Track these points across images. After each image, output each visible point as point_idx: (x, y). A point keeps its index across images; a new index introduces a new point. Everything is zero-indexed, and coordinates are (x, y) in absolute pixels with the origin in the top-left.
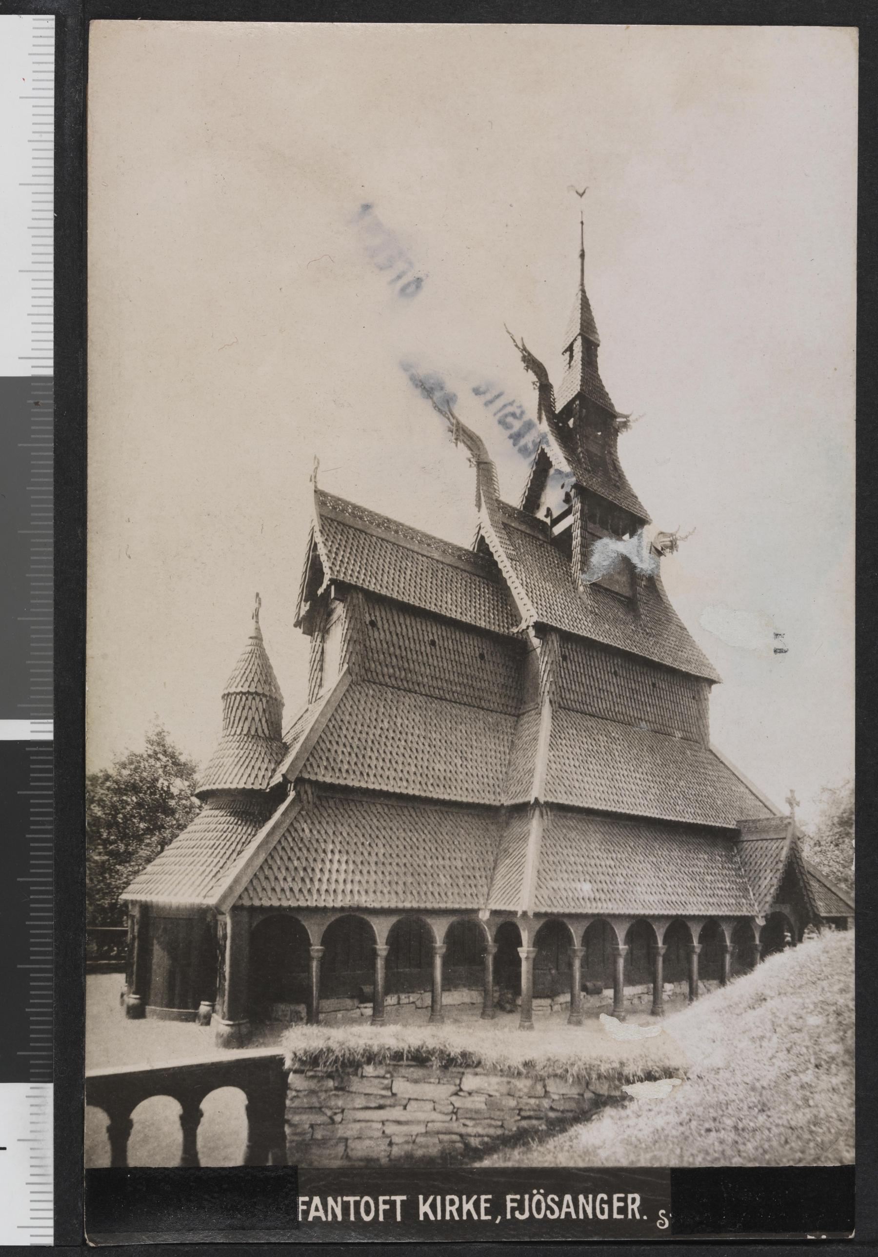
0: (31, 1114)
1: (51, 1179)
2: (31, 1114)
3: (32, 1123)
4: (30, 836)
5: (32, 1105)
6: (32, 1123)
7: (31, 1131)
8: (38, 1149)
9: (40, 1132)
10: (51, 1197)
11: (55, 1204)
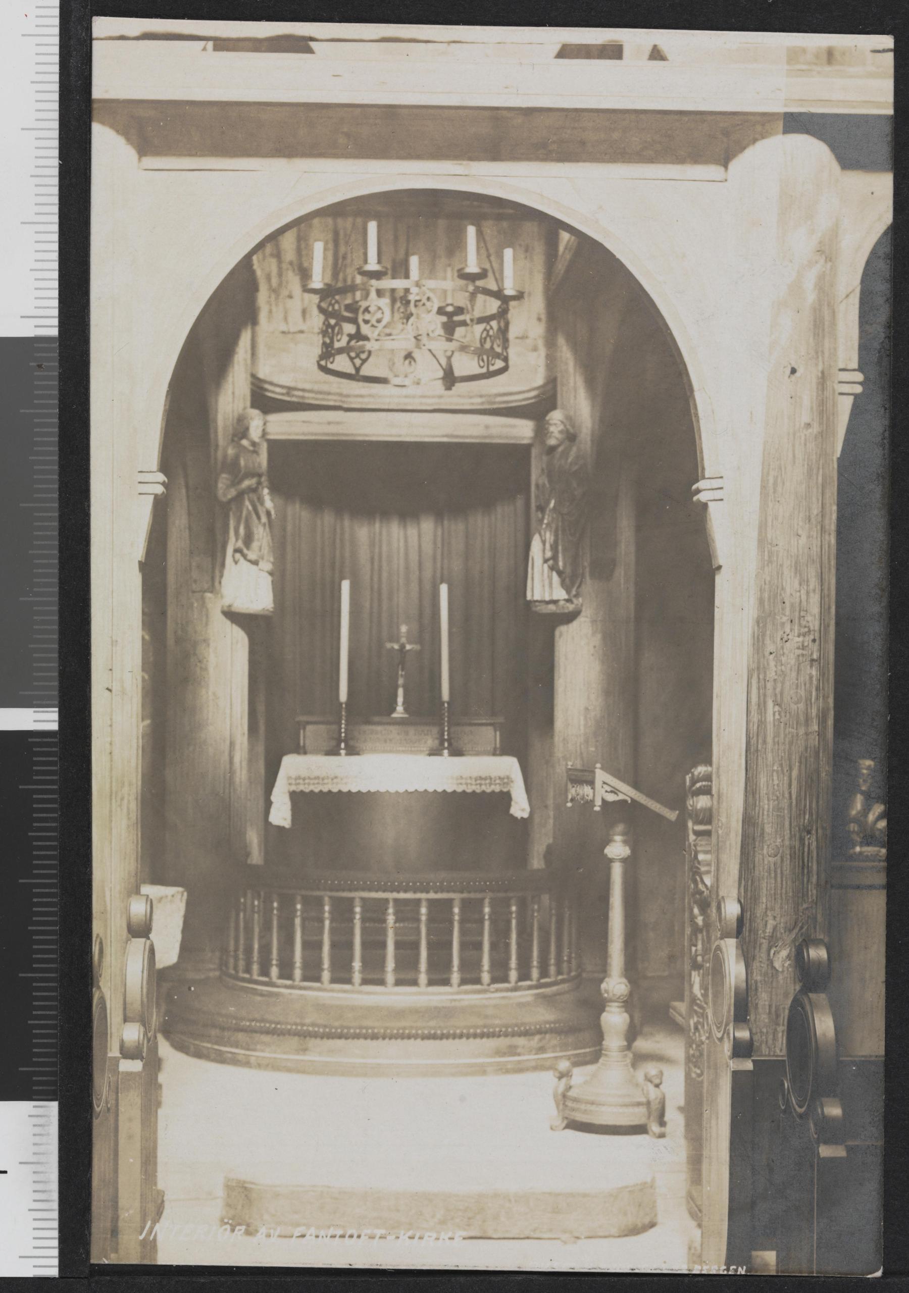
0: (34, 1135)
1: (55, 1205)
2: (34, 1135)
3: (35, 1144)
4: (33, 834)
5: (34, 1126)
6: (35, 1144)
7: (34, 1154)
8: (42, 1172)
9: (43, 1154)
10: (56, 1224)
11: (60, 1232)
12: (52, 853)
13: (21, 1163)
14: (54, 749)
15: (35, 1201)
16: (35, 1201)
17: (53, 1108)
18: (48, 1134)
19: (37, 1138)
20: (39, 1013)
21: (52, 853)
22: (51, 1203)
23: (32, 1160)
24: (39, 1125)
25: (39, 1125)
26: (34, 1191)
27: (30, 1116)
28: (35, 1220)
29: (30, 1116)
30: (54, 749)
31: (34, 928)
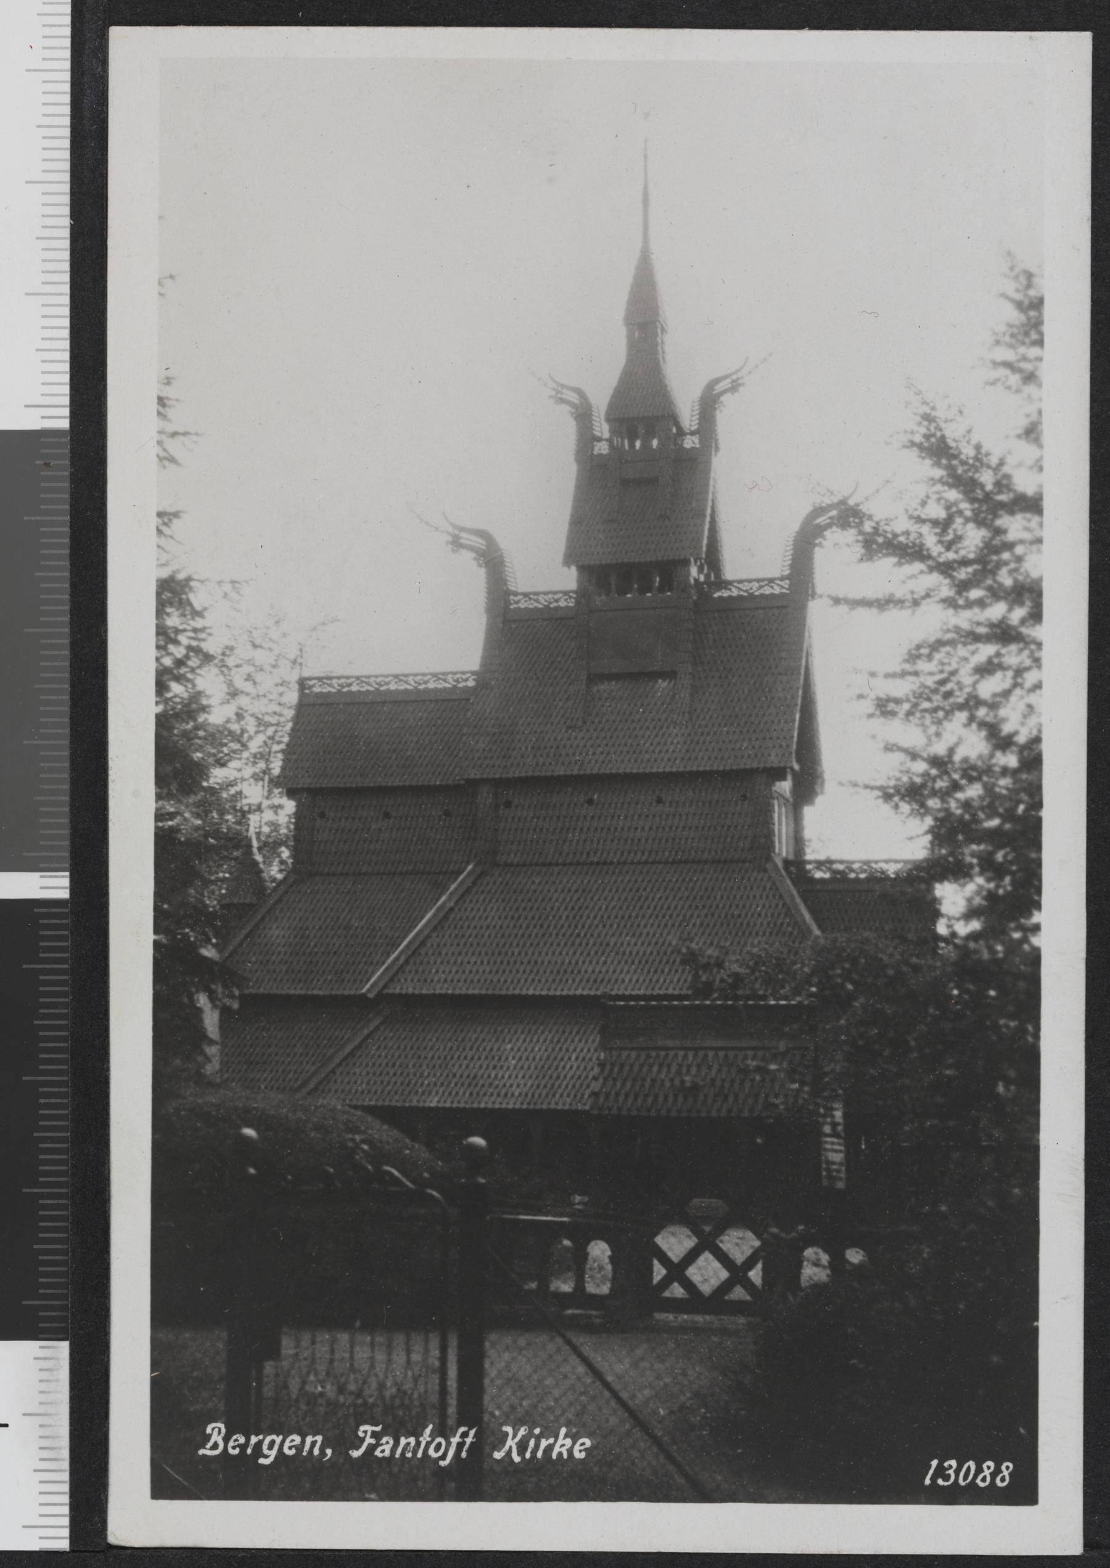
0: (41, 1381)
1: (66, 1465)
2: (41, 1381)
3: (41, 1392)
4: (40, 1022)
5: (41, 1370)
6: (41, 1392)
7: (41, 1403)
9: (51, 1403)
10: (66, 1488)
11: (71, 1497)
12: (62, 1045)
13: (24, 1415)
14: (64, 921)
15: (41, 1460)
16: (41, 1460)
17: (64, 1347)
18: (57, 1380)
19: (44, 1384)
20: (46, 1235)
21: (62, 1045)
22: (61, 1463)
23: (38, 1412)
24: (46, 1370)
25: (46, 1370)
26: (41, 1448)
27: (35, 1359)
28: (41, 1482)
29: (35, 1359)
30: (64, 921)
31: (41, 1134)
